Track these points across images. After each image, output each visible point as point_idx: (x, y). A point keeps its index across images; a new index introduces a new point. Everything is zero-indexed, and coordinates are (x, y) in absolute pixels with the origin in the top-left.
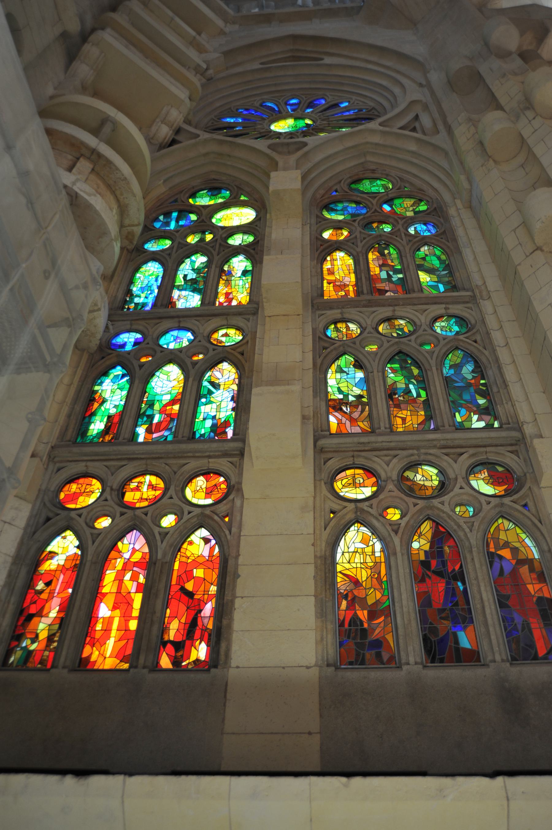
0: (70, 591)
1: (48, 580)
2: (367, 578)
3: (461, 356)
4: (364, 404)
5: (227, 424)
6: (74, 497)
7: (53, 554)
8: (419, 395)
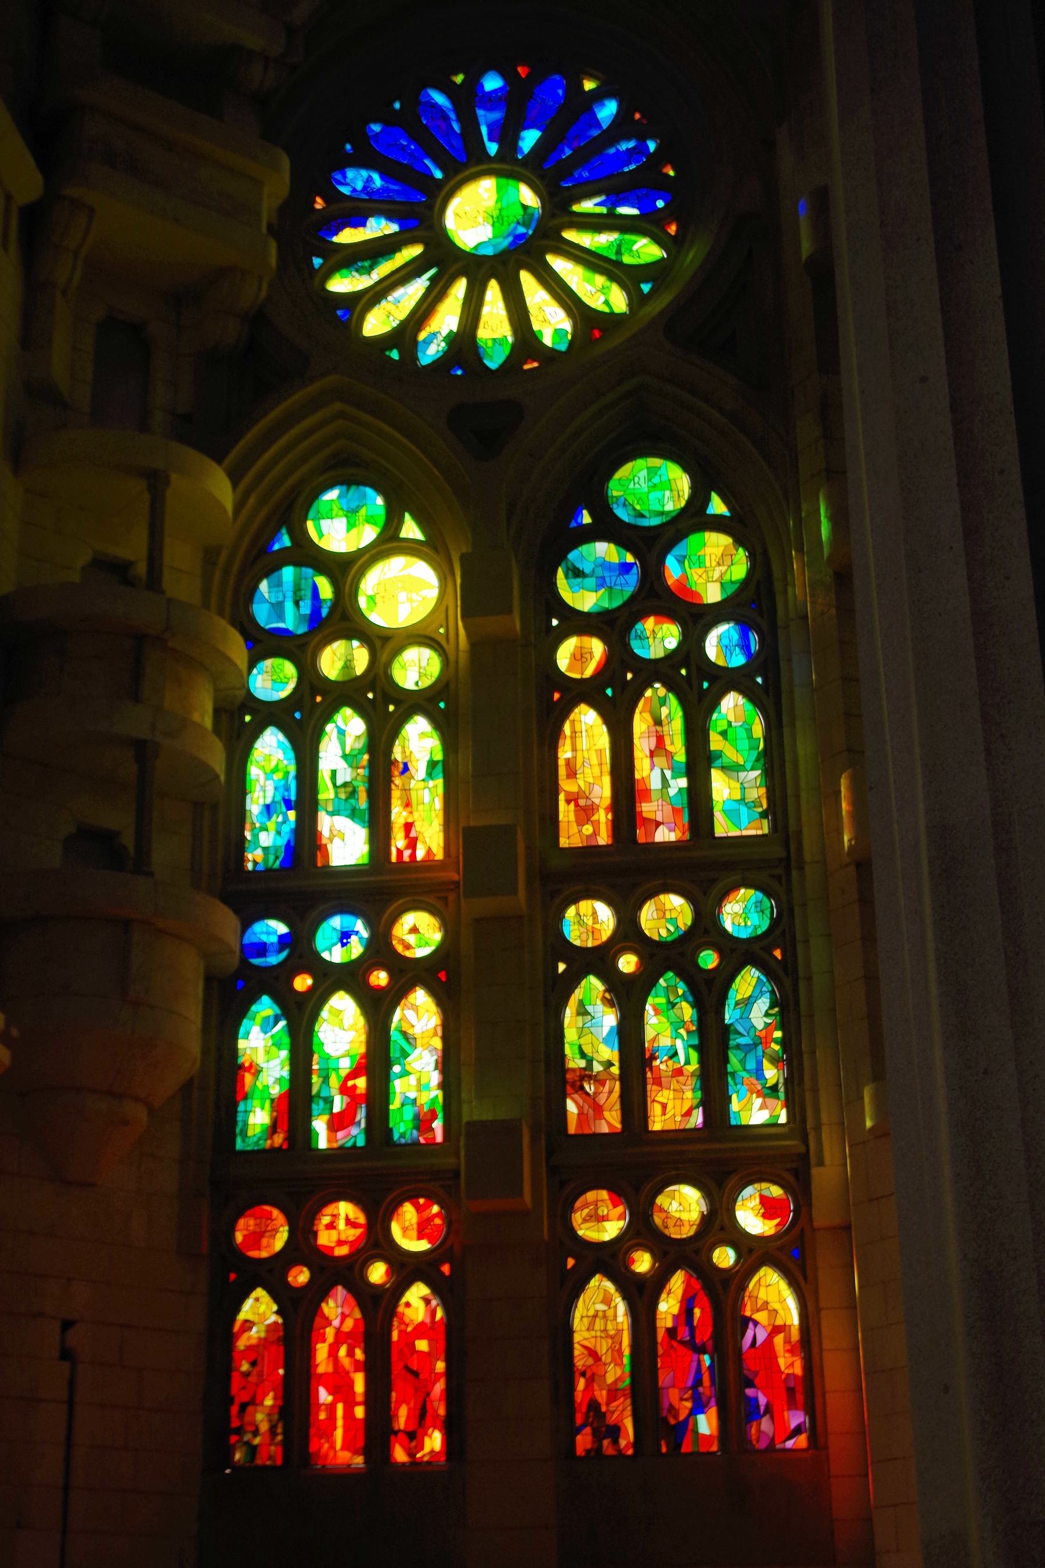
0: (281, 1371)
1: (251, 1360)
2: (607, 1350)
3: (754, 981)
4: (612, 1077)
5: (433, 1114)
6: (255, 1239)
7: (248, 1325)
8: (688, 1062)
